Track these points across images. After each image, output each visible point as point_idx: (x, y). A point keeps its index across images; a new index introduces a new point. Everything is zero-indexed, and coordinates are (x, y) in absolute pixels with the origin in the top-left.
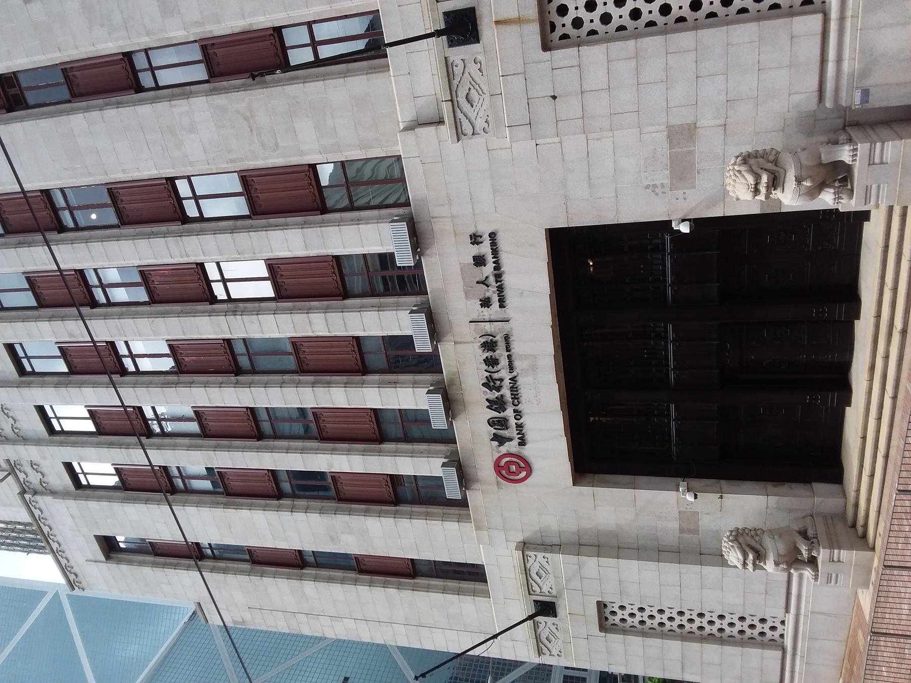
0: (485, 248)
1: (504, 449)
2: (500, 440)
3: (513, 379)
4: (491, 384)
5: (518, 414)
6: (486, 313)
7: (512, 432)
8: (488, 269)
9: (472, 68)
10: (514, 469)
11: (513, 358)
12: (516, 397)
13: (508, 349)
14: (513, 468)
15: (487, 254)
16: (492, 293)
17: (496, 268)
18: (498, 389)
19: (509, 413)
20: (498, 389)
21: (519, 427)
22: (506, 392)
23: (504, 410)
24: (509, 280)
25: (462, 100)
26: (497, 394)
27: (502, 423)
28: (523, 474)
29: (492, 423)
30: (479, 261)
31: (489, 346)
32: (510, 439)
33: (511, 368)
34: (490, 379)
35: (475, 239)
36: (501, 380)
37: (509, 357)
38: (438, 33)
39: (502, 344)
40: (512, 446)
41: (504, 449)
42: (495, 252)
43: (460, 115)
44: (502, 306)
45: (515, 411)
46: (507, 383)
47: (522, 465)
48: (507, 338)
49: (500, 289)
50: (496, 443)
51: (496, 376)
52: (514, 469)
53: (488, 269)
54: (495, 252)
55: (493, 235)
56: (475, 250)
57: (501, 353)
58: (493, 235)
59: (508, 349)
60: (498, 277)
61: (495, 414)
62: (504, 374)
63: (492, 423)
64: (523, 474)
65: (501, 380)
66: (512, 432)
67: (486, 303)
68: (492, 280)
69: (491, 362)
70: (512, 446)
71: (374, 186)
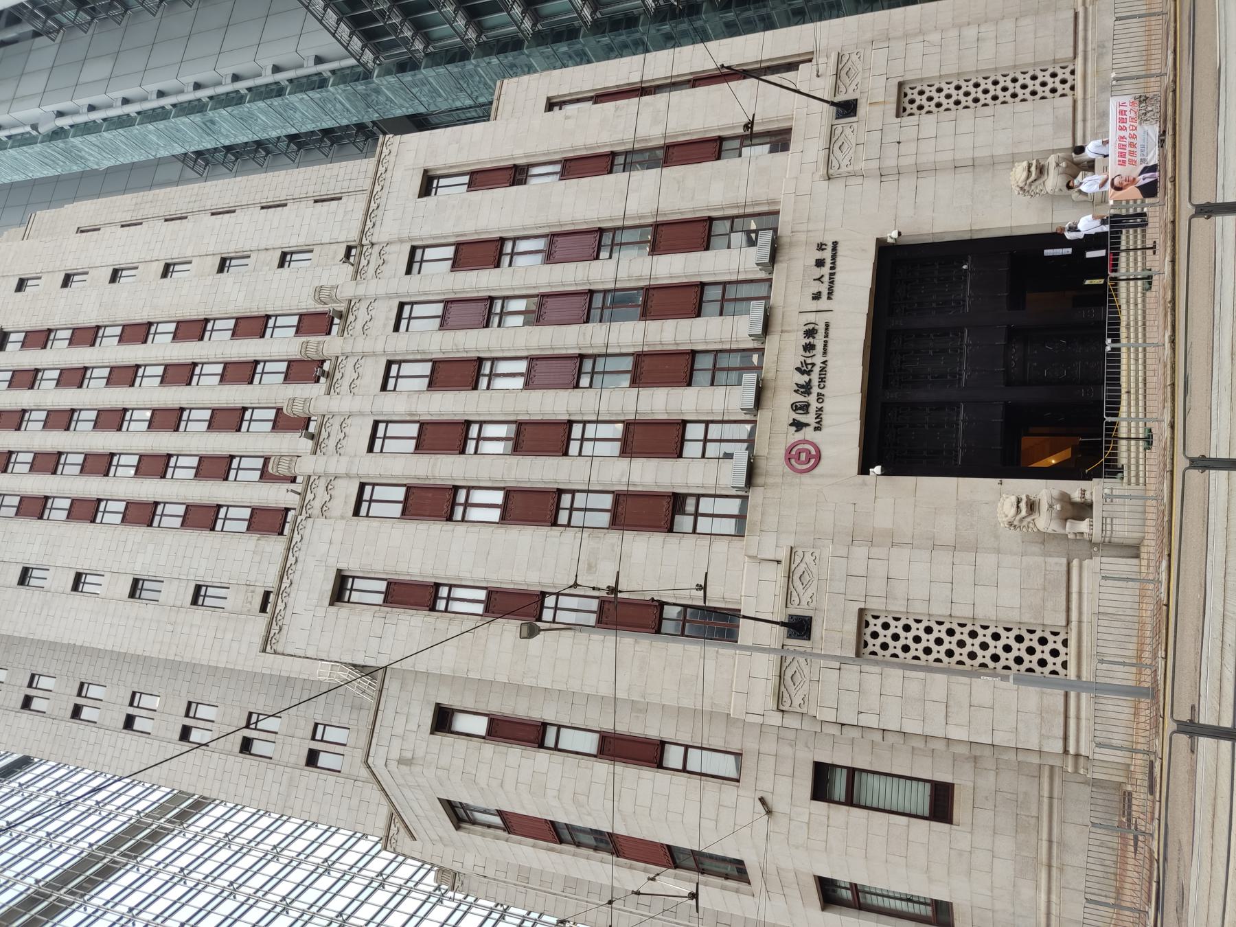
0: (827, 255)
2: (799, 426)
4: (804, 370)
5: (820, 397)
6: (815, 305)
7: (810, 418)
8: (826, 270)
9: (848, 131)
10: (805, 459)
12: (822, 380)
13: (826, 336)
14: (803, 456)
15: (828, 257)
16: (824, 289)
17: (832, 268)
18: (809, 373)
19: (812, 399)
20: (809, 373)
21: (821, 410)
22: (815, 377)
23: (809, 393)
24: (837, 278)
25: (836, 147)
26: (806, 378)
27: (805, 408)
28: (813, 461)
29: (796, 407)
30: (820, 263)
31: (810, 333)
32: (807, 425)
33: (825, 353)
35: (821, 247)
36: (813, 365)
37: (826, 342)
38: (832, 104)
39: (821, 331)
41: (799, 436)
42: (834, 257)
43: (832, 157)
44: (829, 298)
45: (819, 394)
46: (817, 369)
47: (813, 452)
48: (827, 326)
49: (832, 282)
50: (794, 428)
51: (809, 361)
52: (805, 459)
53: (826, 270)
54: (834, 257)
55: (835, 244)
56: (819, 255)
57: (819, 341)
58: (835, 244)
59: (826, 336)
60: (832, 274)
61: (800, 398)
62: (818, 360)
63: (796, 407)
64: (813, 461)
65: (813, 365)
66: (810, 418)
67: (817, 296)
68: (826, 279)
69: (809, 347)
70: (808, 433)
71: (761, 224)
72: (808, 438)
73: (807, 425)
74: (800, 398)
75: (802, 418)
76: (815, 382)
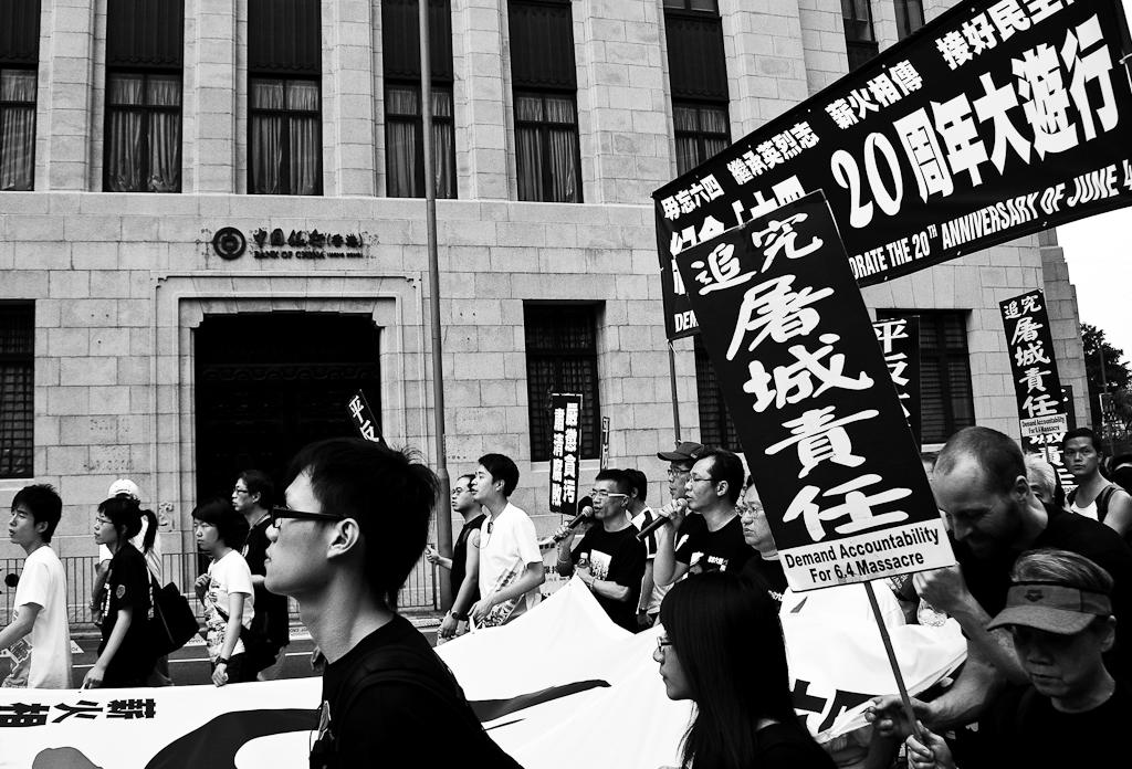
1: (248, 236)
2: (260, 237)
3: (321, 256)
4: (317, 239)
7: (268, 249)
11: (341, 259)
13: (350, 255)
14: (230, 244)
19: (287, 248)
20: (311, 243)
29: (278, 232)
31: (352, 242)
34: (321, 237)
37: (342, 255)
39: (352, 251)
40: (251, 247)
45: (291, 253)
48: (359, 256)
57: (344, 250)
59: (350, 255)
61: (287, 235)
63: (278, 232)
69: (337, 241)
70: (251, 247)
72: (249, 247)
73: (261, 247)
74: (287, 235)
75: (268, 239)
76: (302, 250)
